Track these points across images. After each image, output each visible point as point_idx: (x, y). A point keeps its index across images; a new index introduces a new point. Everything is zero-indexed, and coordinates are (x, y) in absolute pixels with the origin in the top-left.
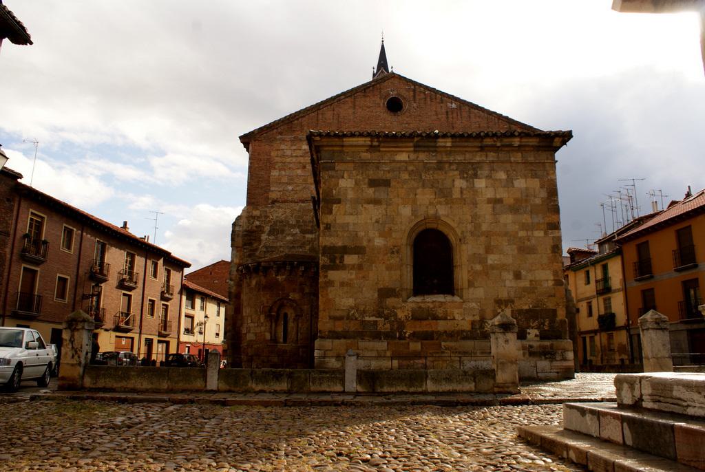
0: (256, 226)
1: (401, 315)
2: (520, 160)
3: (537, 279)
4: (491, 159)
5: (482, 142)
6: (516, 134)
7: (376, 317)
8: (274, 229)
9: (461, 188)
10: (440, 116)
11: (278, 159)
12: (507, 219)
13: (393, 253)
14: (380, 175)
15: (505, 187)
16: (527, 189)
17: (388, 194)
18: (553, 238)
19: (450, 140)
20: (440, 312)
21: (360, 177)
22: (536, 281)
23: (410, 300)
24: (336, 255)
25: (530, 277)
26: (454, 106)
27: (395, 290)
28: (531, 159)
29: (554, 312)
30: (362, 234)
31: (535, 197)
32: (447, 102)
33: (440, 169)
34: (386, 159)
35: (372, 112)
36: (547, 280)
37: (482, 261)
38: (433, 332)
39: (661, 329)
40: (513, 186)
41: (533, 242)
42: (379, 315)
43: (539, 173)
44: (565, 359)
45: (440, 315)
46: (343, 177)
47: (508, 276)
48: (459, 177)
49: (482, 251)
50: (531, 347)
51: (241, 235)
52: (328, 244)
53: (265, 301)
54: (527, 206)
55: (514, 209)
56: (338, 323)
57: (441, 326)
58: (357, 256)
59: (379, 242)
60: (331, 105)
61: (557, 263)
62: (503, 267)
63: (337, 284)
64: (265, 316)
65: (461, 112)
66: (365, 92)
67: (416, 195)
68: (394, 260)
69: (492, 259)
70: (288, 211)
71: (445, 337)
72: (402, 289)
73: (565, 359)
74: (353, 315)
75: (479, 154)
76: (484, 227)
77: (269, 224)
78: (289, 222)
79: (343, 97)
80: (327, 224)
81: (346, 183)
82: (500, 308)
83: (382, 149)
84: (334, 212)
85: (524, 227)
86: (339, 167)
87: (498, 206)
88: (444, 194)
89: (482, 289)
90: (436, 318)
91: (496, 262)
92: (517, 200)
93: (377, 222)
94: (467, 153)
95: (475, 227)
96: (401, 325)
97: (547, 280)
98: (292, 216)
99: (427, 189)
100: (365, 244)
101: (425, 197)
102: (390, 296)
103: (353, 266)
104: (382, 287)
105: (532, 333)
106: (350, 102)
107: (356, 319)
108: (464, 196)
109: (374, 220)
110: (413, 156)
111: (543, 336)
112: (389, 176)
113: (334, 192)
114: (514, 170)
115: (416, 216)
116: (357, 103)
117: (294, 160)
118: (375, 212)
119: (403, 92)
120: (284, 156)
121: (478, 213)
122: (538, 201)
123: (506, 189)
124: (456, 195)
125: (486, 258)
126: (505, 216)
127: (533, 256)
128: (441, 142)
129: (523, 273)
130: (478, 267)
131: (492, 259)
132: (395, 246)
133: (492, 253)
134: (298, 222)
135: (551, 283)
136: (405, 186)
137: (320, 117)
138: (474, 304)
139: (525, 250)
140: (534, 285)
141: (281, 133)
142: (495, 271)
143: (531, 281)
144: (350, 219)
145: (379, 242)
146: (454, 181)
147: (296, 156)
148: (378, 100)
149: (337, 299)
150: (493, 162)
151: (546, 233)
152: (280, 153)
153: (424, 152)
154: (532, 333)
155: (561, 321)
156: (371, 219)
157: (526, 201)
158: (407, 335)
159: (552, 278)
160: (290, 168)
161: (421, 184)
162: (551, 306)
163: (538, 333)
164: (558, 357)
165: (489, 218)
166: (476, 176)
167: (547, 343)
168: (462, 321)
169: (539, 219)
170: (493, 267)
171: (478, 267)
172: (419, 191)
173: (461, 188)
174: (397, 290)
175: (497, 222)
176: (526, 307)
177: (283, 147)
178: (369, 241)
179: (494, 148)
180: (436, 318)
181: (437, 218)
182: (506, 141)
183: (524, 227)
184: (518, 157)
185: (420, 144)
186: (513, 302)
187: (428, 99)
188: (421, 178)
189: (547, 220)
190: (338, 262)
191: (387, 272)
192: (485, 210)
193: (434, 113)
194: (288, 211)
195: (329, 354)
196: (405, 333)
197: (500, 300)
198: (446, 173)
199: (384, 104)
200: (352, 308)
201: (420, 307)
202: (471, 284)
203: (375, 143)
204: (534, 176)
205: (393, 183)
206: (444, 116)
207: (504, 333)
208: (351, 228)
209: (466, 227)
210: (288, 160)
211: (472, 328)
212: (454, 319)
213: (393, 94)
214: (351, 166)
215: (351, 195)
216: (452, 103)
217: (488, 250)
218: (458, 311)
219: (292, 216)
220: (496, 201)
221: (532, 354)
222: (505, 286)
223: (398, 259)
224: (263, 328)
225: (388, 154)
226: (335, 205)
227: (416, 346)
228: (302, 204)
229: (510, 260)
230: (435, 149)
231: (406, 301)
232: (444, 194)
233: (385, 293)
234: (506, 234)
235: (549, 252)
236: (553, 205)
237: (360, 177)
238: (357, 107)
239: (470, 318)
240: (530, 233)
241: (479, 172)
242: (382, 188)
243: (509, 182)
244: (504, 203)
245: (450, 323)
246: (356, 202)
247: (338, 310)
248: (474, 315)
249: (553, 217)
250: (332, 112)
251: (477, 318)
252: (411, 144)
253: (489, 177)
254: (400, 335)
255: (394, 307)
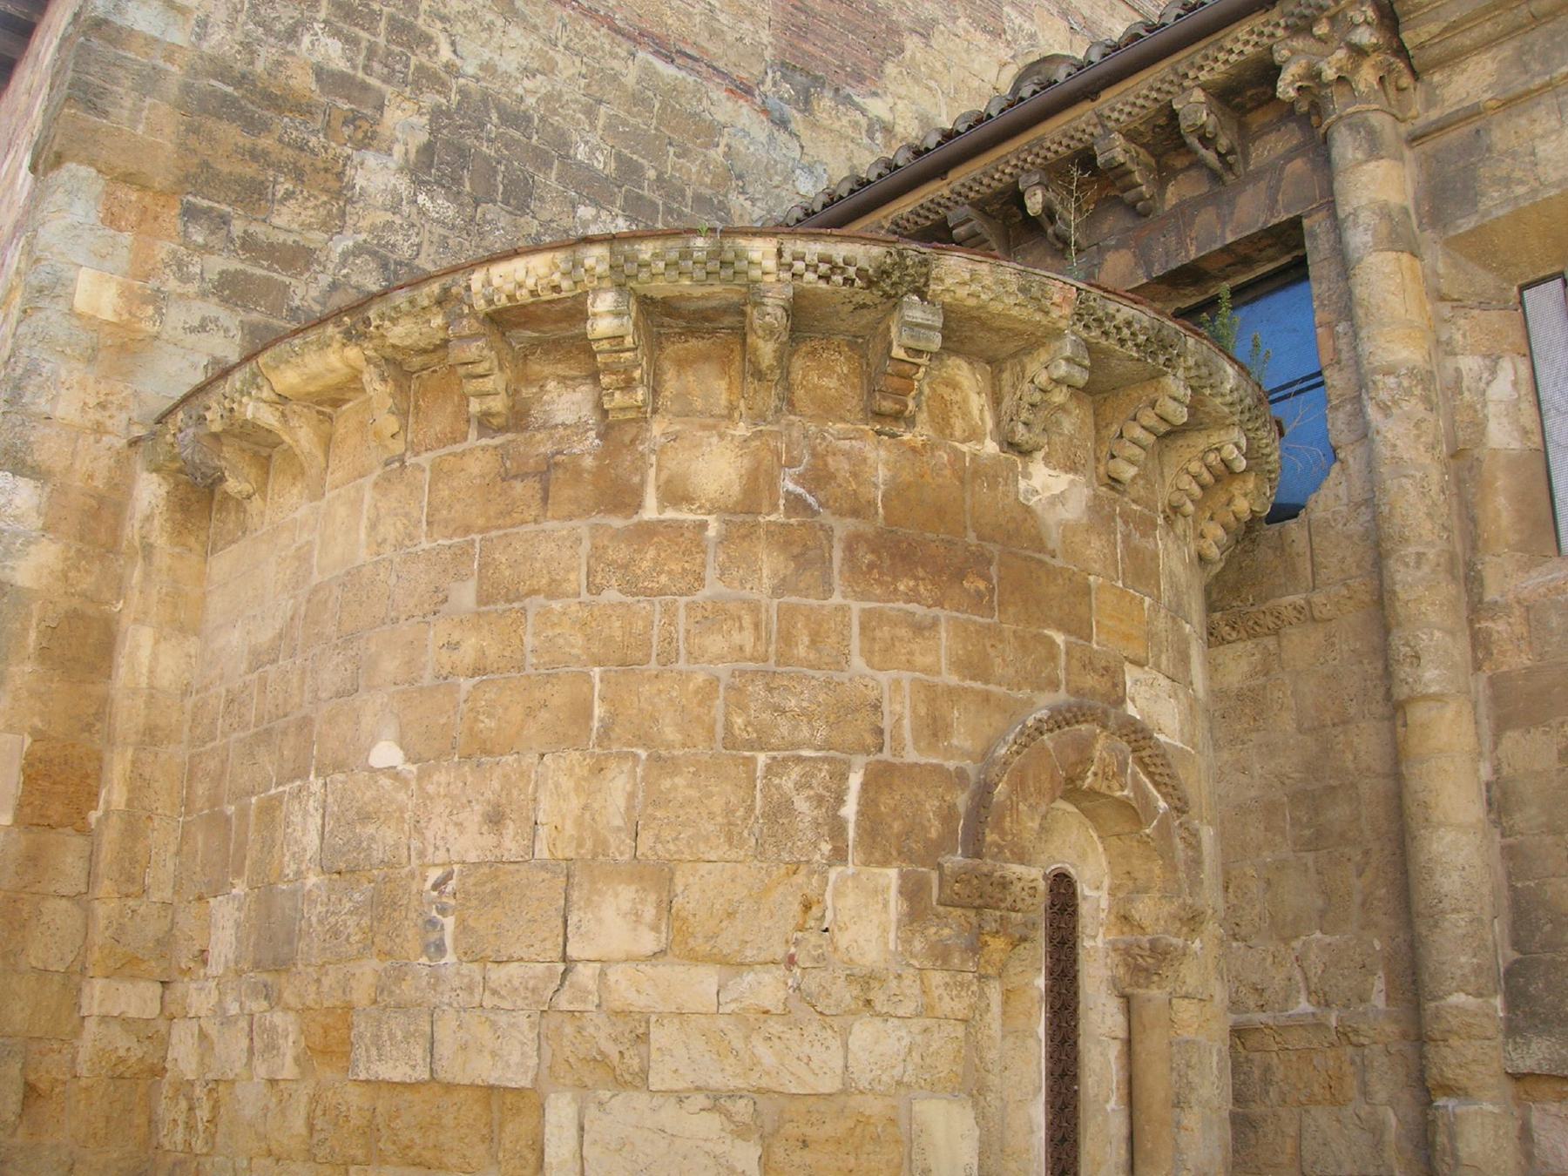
0: (320, 73)
8: (462, 152)
51: (172, 88)
53: (901, 712)
64: (913, 891)
70: (567, 66)
77: (430, 99)
78: (562, 142)
98: (590, 112)
134: (629, 170)
194: (567, 66)
219: (590, 112)
224: (877, 1046)
228: (660, 65)
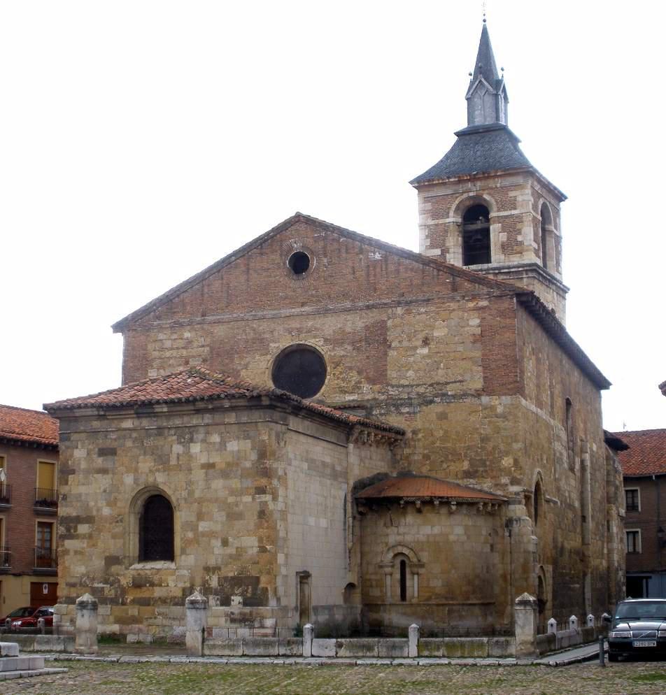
1: (124, 582)
2: (233, 420)
3: (243, 546)
4: (206, 421)
5: (194, 405)
6: (222, 396)
7: (104, 584)
9: (178, 454)
10: (358, 274)
11: (156, 354)
12: (218, 484)
13: (117, 522)
14: (108, 444)
15: (217, 451)
16: (239, 451)
17: (114, 463)
18: (261, 502)
19: (164, 405)
20: (156, 579)
21: (90, 447)
22: (241, 548)
23: (133, 567)
24: (71, 525)
25: (237, 543)
26: (378, 256)
27: (118, 557)
28: (244, 419)
29: (258, 579)
30: (92, 504)
31: (246, 460)
32: (368, 251)
33: (160, 434)
34: (114, 425)
35: (270, 276)
36: (253, 547)
37: (194, 528)
38: (150, 598)
39: (194, 608)
40: (225, 450)
41: (241, 507)
42: (106, 582)
43: (252, 434)
44: (262, 627)
45: (156, 582)
46: (77, 448)
47: (217, 543)
48: (176, 442)
49: (193, 519)
50: (232, 613)
52: (65, 514)
54: (237, 470)
55: (225, 474)
56: (73, 589)
57: (158, 592)
58: (87, 525)
59: (106, 511)
60: (219, 271)
61: (263, 528)
62: (211, 534)
63: (72, 553)
65: (387, 265)
66: (261, 248)
67: (138, 463)
68: (118, 529)
69: (203, 526)
71: (159, 603)
72: (125, 557)
73: (262, 627)
74: (85, 582)
75: (196, 416)
76: (197, 494)
79: (233, 258)
80: (64, 495)
81: (79, 453)
82: (208, 575)
83: (108, 417)
84: (69, 483)
85: (233, 492)
86: (74, 437)
87: (211, 471)
88: (162, 461)
89: (192, 556)
90: (152, 585)
91: (206, 529)
92: (228, 464)
93: (105, 491)
94: (184, 416)
95: (188, 494)
96: (124, 591)
97: (253, 547)
99: (148, 457)
100: (94, 513)
101: (146, 464)
102: (115, 564)
103: (85, 535)
104: (108, 554)
105: (237, 599)
106: (242, 266)
107: (87, 585)
108: (180, 463)
109: (102, 490)
110: (137, 422)
111: (245, 603)
112: (115, 444)
113: (70, 462)
114: (228, 432)
115: (138, 485)
116: (252, 265)
117: (174, 353)
118: (104, 481)
119: (309, 242)
120: (162, 349)
121: (192, 480)
122: (248, 464)
123: (219, 452)
124: (173, 462)
125: (198, 526)
126: (216, 481)
127: (241, 522)
128: (158, 409)
129: (230, 539)
130: (190, 535)
131: (203, 526)
132: (119, 515)
133: (203, 520)
135: (256, 550)
136: (129, 454)
137: (206, 290)
138: (185, 571)
139: (234, 516)
140: (240, 552)
141: (159, 318)
142: (204, 539)
143: (237, 548)
144: (82, 489)
145: (106, 511)
146: (172, 446)
147: (178, 348)
148: (276, 257)
149: (72, 567)
150: (208, 425)
151: (254, 499)
152: (157, 345)
153: (146, 417)
154: (237, 599)
155: (263, 588)
156: (100, 488)
157: (237, 464)
158: (128, 601)
159: (257, 544)
160: (170, 365)
161: (142, 452)
162: (254, 574)
163: (241, 601)
164: (257, 624)
165: (201, 484)
166: (191, 440)
167: (247, 610)
168: (174, 586)
169: (249, 483)
170: (203, 534)
171: (190, 535)
172: (142, 457)
173: (178, 454)
174: (121, 557)
175: (209, 488)
176: (231, 574)
177: (161, 336)
178: (98, 510)
179: (206, 410)
180: (152, 585)
181: (156, 487)
182: (217, 403)
183: (233, 492)
184: (231, 418)
185: (140, 411)
186: (219, 569)
187: (343, 251)
188: (143, 445)
189: (257, 484)
190: (72, 531)
191: (113, 541)
192: (198, 475)
193: (350, 270)
195: (66, 617)
196: (127, 599)
197: (209, 567)
198: (165, 438)
199: (285, 264)
200: (83, 575)
201: (139, 574)
202: (183, 552)
203: (102, 413)
204: (247, 437)
205: (119, 452)
206: (363, 273)
207: (81, 609)
208: (83, 498)
209: (181, 494)
210: (168, 354)
211: (183, 595)
212: (168, 586)
213: (297, 247)
214: (83, 435)
215: (83, 465)
216: (374, 254)
217: (200, 516)
218: (171, 575)
220: (209, 466)
221: (233, 621)
222: (213, 553)
223: (121, 528)
225: (116, 422)
226: (70, 476)
227: (134, 611)
229: (218, 528)
230: (156, 415)
231: (128, 569)
232: (162, 461)
233: (112, 560)
234: (216, 500)
235: (256, 517)
236: (262, 468)
237: (90, 447)
238: (251, 272)
239: (181, 585)
240: (238, 499)
241: (195, 437)
242: (110, 457)
243: (223, 444)
244: (217, 467)
245: (164, 589)
246: (88, 472)
247: (73, 577)
248: (185, 582)
249: (262, 480)
250: (220, 282)
251: (188, 585)
252: (132, 412)
253: (204, 441)
254: (123, 600)
255: (118, 575)
